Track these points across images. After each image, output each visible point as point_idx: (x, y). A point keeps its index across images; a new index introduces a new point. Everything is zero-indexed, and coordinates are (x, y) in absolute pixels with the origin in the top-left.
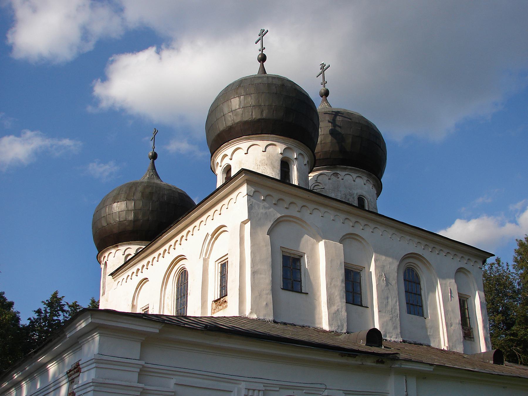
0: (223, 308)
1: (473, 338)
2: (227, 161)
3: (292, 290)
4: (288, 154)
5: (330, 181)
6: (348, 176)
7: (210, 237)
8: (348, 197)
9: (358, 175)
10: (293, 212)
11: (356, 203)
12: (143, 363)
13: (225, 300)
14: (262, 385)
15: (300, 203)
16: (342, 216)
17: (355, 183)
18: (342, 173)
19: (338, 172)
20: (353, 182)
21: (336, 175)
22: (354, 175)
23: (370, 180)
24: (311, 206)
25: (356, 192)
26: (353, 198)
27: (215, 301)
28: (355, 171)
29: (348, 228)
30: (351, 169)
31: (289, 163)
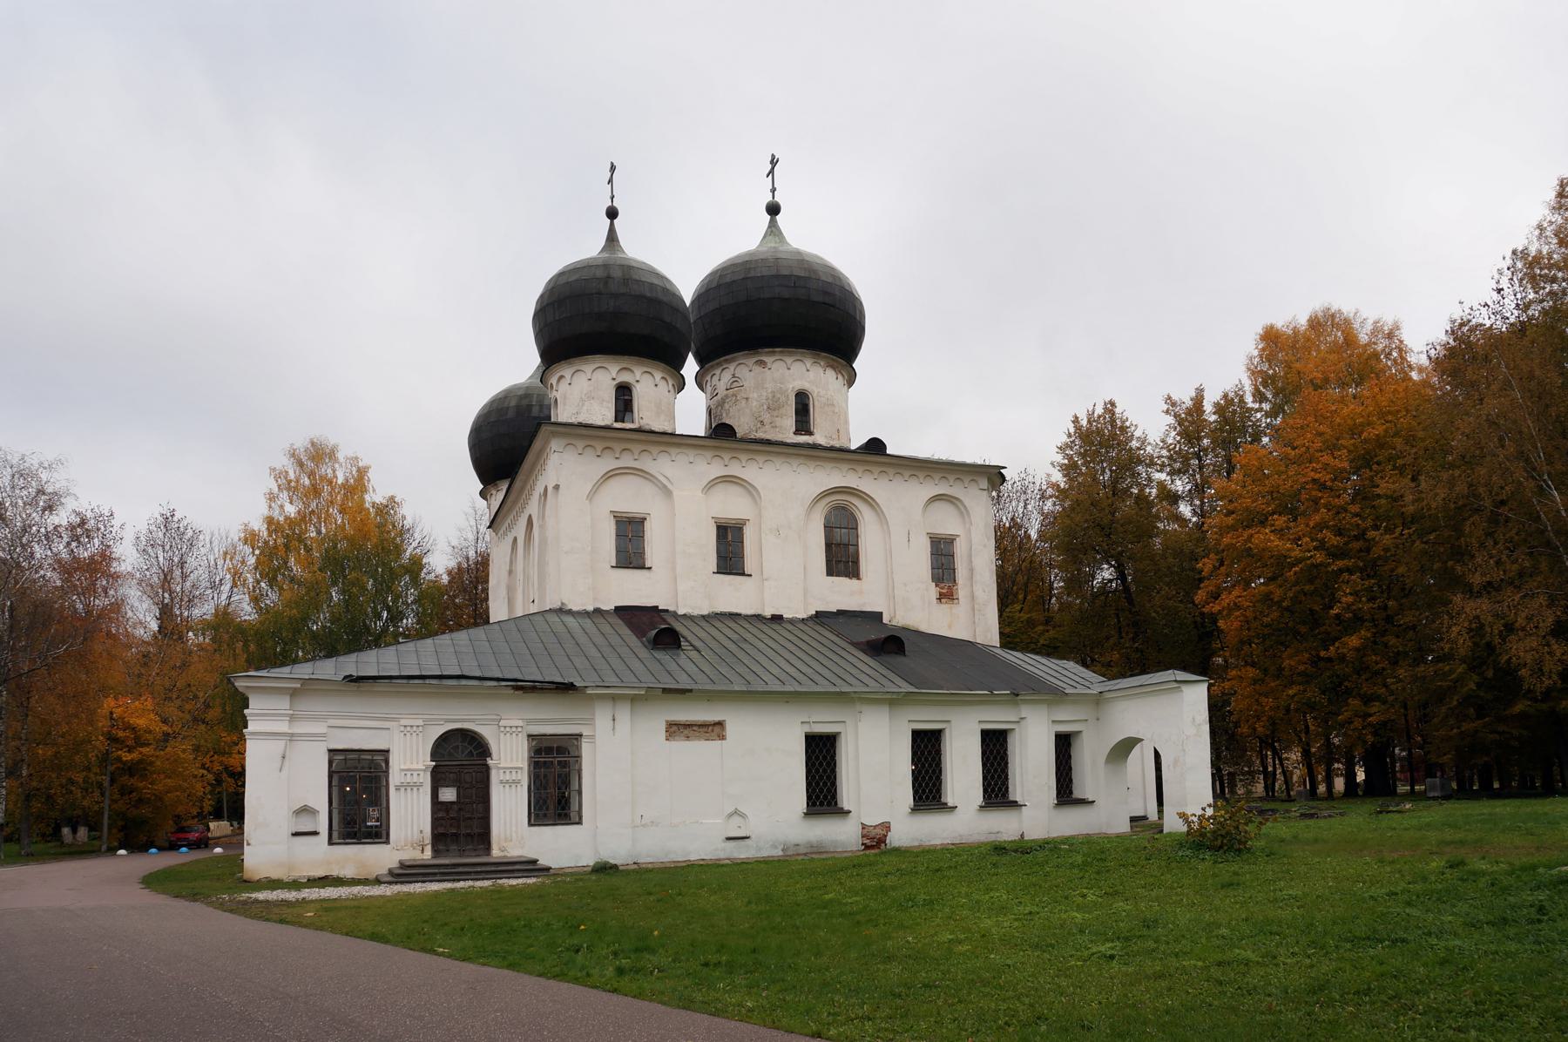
4: (625, 377)
5: (752, 373)
10: (627, 461)
12: (291, 712)
14: (421, 721)
16: (709, 454)
17: (791, 371)
18: (768, 360)
19: (762, 358)
21: (762, 363)
22: (789, 360)
23: (819, 361)
24: (655, 450)
25: (791, 386)
28: (790, 354)
29: (716, 469)
30: (781, 352)
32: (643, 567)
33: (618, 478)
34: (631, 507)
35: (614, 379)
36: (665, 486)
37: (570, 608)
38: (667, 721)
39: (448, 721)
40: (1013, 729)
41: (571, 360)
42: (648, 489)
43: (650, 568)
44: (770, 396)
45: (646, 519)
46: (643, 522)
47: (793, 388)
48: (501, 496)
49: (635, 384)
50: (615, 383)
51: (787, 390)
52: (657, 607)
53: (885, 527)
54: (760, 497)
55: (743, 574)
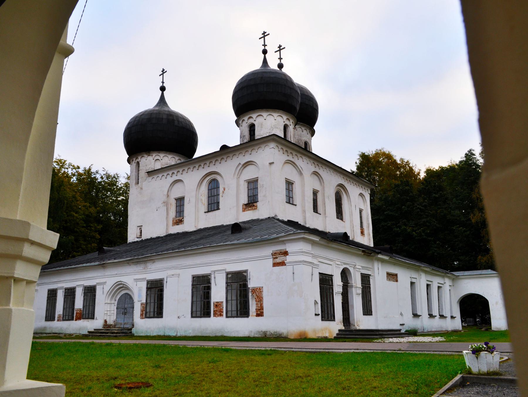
0: (252, 209)
1: (364, 235)
2: (251, 121)
3: (289, 203)
4: (287, 122)
6: (300, 128)
7: (240, 166)
8: (300, 142)
9: (305, 128)
11: (303, 147)
13: (253, 205)
15: (294, 153)
16: (312, 161)
20: (302, 132)
22: (303, 128)
25: (303, 139)
26: (302, 143)
27: (245, 204)
28: (304, 126)
30: (301, 124)
31: (286, 128)
32: (293, 204)
33: (290, 165)
34: (291, 178)
35: (284, 122)
36: (300, 171)
37: (279, 218)
38: (387, 272)
39: (345, 264)
40: (442, 287)
41: (269, 109)
42: (295, 171)
43: (296, 205)
44: (297, 141)
45: (293, 184)
46: (292, 185)
47: (304, 140)
48: (183, 161)
49: (289, 126)
50: (284, 124)
51: (302, 140)
52: (298, 222)
53: (349, 202)
54: (324, 183)
55: (317, 213)
